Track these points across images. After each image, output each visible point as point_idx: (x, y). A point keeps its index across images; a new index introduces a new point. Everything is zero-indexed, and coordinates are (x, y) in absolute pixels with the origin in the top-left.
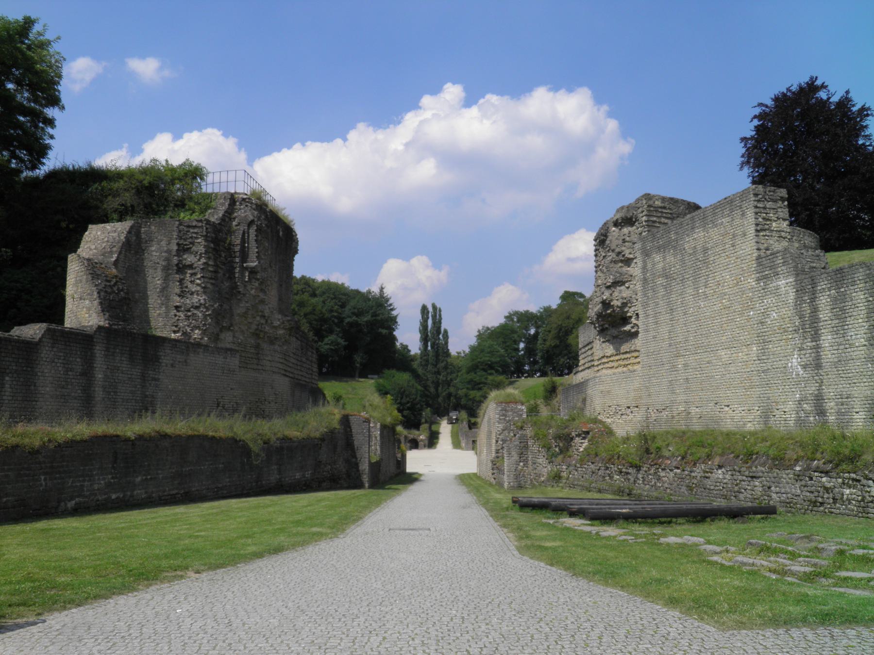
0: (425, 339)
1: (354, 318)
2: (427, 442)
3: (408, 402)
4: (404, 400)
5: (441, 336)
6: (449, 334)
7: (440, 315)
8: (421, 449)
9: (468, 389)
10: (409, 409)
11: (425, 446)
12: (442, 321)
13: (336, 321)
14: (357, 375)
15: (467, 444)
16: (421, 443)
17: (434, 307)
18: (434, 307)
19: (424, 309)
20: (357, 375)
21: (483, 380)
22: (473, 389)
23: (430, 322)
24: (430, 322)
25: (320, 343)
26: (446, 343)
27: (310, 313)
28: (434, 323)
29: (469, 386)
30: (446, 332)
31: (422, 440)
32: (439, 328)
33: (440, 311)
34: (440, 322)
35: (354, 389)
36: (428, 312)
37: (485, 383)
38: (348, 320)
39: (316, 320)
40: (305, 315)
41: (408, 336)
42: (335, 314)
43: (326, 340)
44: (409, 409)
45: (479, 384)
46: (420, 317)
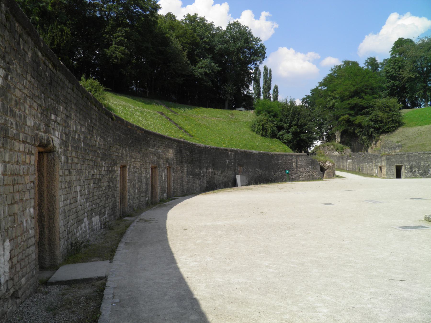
6: (279, 90)
9: (350, 115)
12: (272, 79)
14: (227, 105)
15: (389, 170)
20: (227, 105)
21: (372, 103)
22: (356, 114)
25: (192, 67)
28: (265, 81)
29: (352, 112)
30: (276, 87)
34: (270, 80)
35: (232, 115)
36: (260, 73)
37: (372, 107)
40: (177, 37)
42: (207, 40)
43: (199, 65)
45: (367, 108)
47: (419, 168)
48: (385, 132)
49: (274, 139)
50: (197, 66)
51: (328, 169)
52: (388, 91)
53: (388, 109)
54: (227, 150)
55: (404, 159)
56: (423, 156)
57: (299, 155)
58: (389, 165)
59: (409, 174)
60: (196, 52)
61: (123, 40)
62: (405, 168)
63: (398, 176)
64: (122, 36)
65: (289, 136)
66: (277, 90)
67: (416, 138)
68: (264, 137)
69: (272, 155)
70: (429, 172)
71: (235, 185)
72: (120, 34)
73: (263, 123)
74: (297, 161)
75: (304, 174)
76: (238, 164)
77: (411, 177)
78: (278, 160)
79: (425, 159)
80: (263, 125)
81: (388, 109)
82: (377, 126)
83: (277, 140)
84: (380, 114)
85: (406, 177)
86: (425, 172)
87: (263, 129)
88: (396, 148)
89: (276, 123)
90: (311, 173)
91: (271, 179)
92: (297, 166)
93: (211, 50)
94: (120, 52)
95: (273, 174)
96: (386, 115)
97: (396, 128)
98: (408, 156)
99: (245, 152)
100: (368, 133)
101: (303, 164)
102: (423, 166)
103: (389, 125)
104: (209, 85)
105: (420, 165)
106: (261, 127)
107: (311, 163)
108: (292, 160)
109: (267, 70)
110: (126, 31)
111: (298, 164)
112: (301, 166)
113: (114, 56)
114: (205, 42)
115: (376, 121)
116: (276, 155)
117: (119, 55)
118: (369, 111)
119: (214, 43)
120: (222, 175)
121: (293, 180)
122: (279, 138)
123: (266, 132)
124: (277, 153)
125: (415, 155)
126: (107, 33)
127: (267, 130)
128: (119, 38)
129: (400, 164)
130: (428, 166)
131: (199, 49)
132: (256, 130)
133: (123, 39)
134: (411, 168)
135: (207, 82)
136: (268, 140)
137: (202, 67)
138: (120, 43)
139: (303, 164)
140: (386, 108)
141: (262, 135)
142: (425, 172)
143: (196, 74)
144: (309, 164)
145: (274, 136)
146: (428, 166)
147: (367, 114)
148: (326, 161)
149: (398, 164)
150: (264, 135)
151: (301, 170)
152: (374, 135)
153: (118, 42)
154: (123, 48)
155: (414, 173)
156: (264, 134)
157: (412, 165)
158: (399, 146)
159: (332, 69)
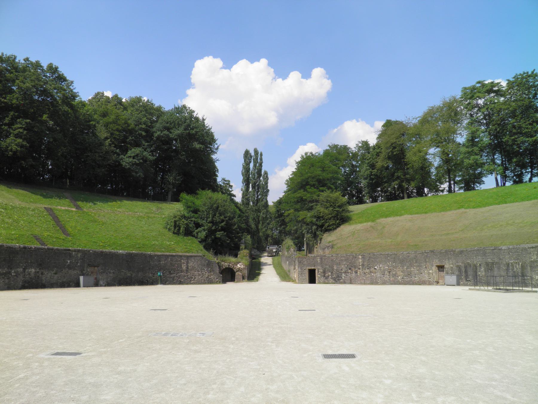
0: (247, 181)
1: (166, 132)
2: (246, 272)
3: (223, 221)
4: (217, 219)
5: (261, 178)
7: (261, 159)
8: (238, 282)
10: (223, 229)
11: (243, 278)
12: (263, 164)
13: (144, 133)
15: (301, 274)
16: (238, 274)
17: (256, 151)
18: (256, 151)
19: (247, 153)
21: (315, 197)
22: (302, 209)
23: (252, 165)
24: (252, 165)
26: (267, 183)
27: (114, 122)
30: (266, 173)
31: (239, 270)
32: (260, 170)
33: (261, 155)
34: (261, 165)
35: (158, 208)
38: (156, 135)
39: (117, 130)
41: (228, 169)
42: (144, 126)
43: (129, 153)
44: (223, 229)
45: (312, 201)
46: (242, 161)
47: (332, 273)
48: (327, 230)
49: (190, 238)
50: (126, 155)
51: (238, 271)
52: (367, 181)
53: (328, 205)
54: (69, 250)
55: (317, 261)
56: (337, 259)
57: (191, 256)
58: (301, 269)
59: (322, 279)
60: (128, 140)
61: (22, 133)
62: (318, 272)
63: (312, 280)
64: (21, 128)
65: (202, 235)
66: (267, 177)
67: (347, 238)
68: (176, 235)
69: (150, 256)
70: (342, 277)
71: (77, 285)
72: (19, 126)
73: (176, 219)
74: (187, 263)
75: (197, 277)
76: (89, 265)
77: (324, 283)
78: (160, 261)
79: (338, 262)
80: (175, 222)
81: (328, 205)
82: (319, 223)
83: (191, 237)
84: (322, 210)
85: (320, 283)
86: (338, 276)
87: (175, 227)
88: (325, 249)
89: (193, 219)
90: (206, 276)
91: (147, 281)
92: (187, 268)
93: (149, 135)
94: (16, 145)
95: (151, 275)
96: (326, 211)
97: (338, 226)
98: (321, 259)
99: (102, 252)
100: (312, 231)
101: (196, 266)
102: (336, 270)
103: (332, 222)
104: (140, 175)
105: (333, 269)
106: (173, 224)
107: (207, 265)
108: (180, 261)
109: (257, 154)
110: (26, 122)
111: (189, 265)
112: (193, 268)
113: (10, 148)
114: (141, 129)
115: (318, 218)
116: (156, 255)
117: (14, 147)
118: (312, 206)
119: (154, 129)
120: (56, 276)
121: (181, 283)
122: (193, 236)
123: (179, 229)
124: (159, 253)
125: (329, 257)
126: (6, 124)
127: (180, 227)
128: (18, 130)
129: (313, 268)
130: (342, 270)
131: (132, 137)
132: (168, 227)
133: (21, 130)
134: (324, 272)
135: (136, 173)
136: (180, 238)
137: (130, 157)
138: (17, 136)
139: (196, 266)
140: (332, 204)
141: (174, 233)
142: (338, 276)
143: (124, 164)
144: (204, 265)
145: (188, 233)
146: (342, 270)
147: (311, 209)
148: (238, 263)
149: (310, 268)
150: (177, 233)
151: (192, 272)
152: (318, 233)
153: (17, 134)
154: (21, 140)
155: (327, 278)
156: (176, 231)
157: (325, 268)
158: (329, 246)
159: (302, 156)
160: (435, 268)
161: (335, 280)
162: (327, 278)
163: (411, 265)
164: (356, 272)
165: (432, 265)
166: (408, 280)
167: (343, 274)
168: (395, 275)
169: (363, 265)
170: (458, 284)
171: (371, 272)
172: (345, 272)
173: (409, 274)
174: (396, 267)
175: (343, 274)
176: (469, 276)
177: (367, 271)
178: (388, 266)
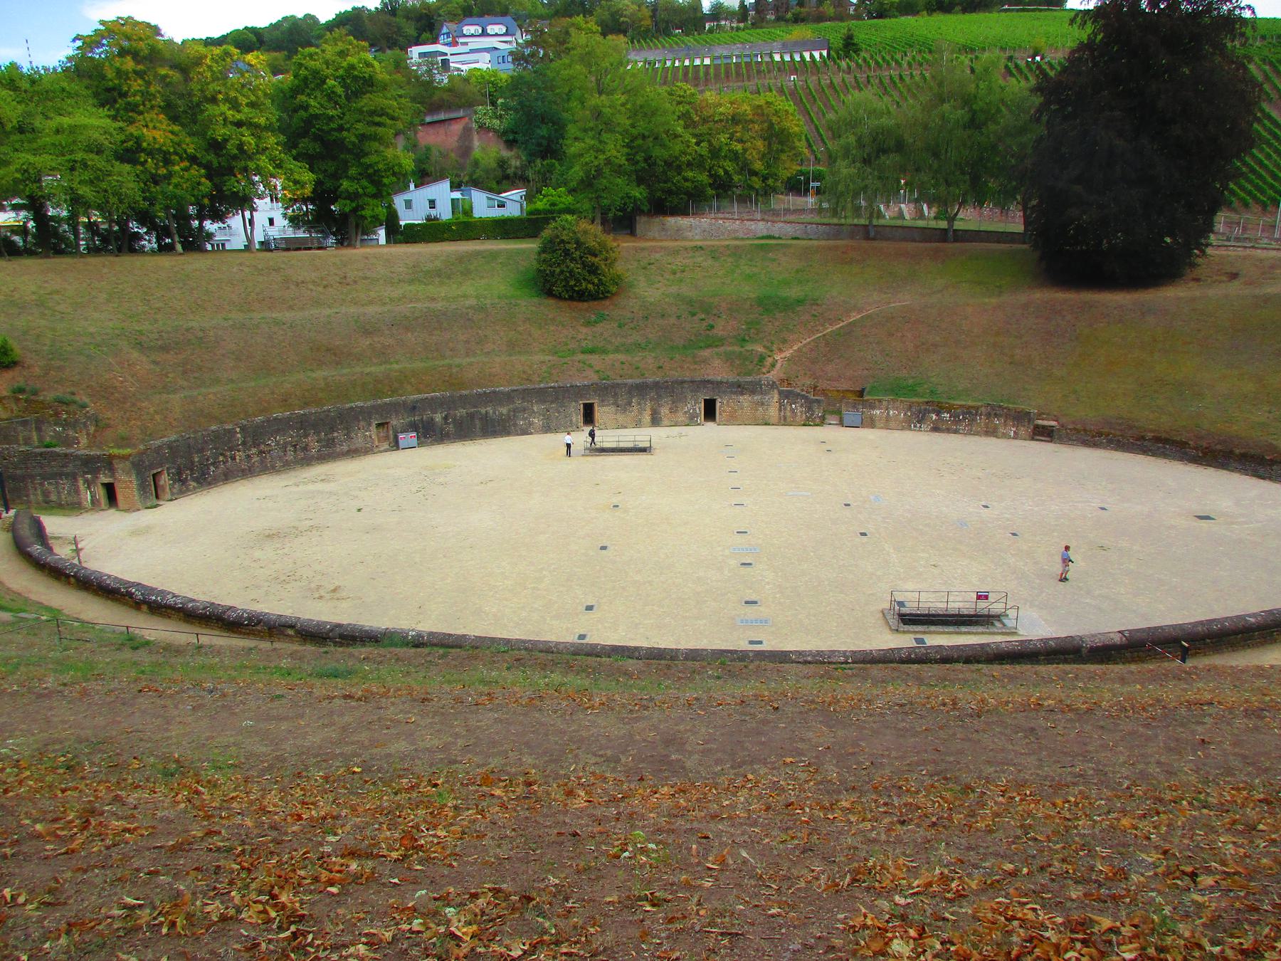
105: (192, 463)
134: (179, 473)
155: (184, 482)
160: (373, 428)
161: (198, 482)
162: (184, 482)
163: (332, 430)
164: (234, 458)
165: (370, 425)
166: (329, 453)
167: (212, 468)
168: (305, 449)
169: (244, 443)
170: (420, 444)
171: (262, 452)
172: (213, 464)
173: (330, 443)
174: (306, 436)
175: (212, 468)
176: (430, 433)
177: (254, 451)
178: (292, 437)
